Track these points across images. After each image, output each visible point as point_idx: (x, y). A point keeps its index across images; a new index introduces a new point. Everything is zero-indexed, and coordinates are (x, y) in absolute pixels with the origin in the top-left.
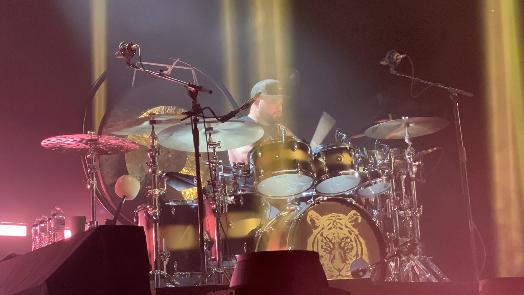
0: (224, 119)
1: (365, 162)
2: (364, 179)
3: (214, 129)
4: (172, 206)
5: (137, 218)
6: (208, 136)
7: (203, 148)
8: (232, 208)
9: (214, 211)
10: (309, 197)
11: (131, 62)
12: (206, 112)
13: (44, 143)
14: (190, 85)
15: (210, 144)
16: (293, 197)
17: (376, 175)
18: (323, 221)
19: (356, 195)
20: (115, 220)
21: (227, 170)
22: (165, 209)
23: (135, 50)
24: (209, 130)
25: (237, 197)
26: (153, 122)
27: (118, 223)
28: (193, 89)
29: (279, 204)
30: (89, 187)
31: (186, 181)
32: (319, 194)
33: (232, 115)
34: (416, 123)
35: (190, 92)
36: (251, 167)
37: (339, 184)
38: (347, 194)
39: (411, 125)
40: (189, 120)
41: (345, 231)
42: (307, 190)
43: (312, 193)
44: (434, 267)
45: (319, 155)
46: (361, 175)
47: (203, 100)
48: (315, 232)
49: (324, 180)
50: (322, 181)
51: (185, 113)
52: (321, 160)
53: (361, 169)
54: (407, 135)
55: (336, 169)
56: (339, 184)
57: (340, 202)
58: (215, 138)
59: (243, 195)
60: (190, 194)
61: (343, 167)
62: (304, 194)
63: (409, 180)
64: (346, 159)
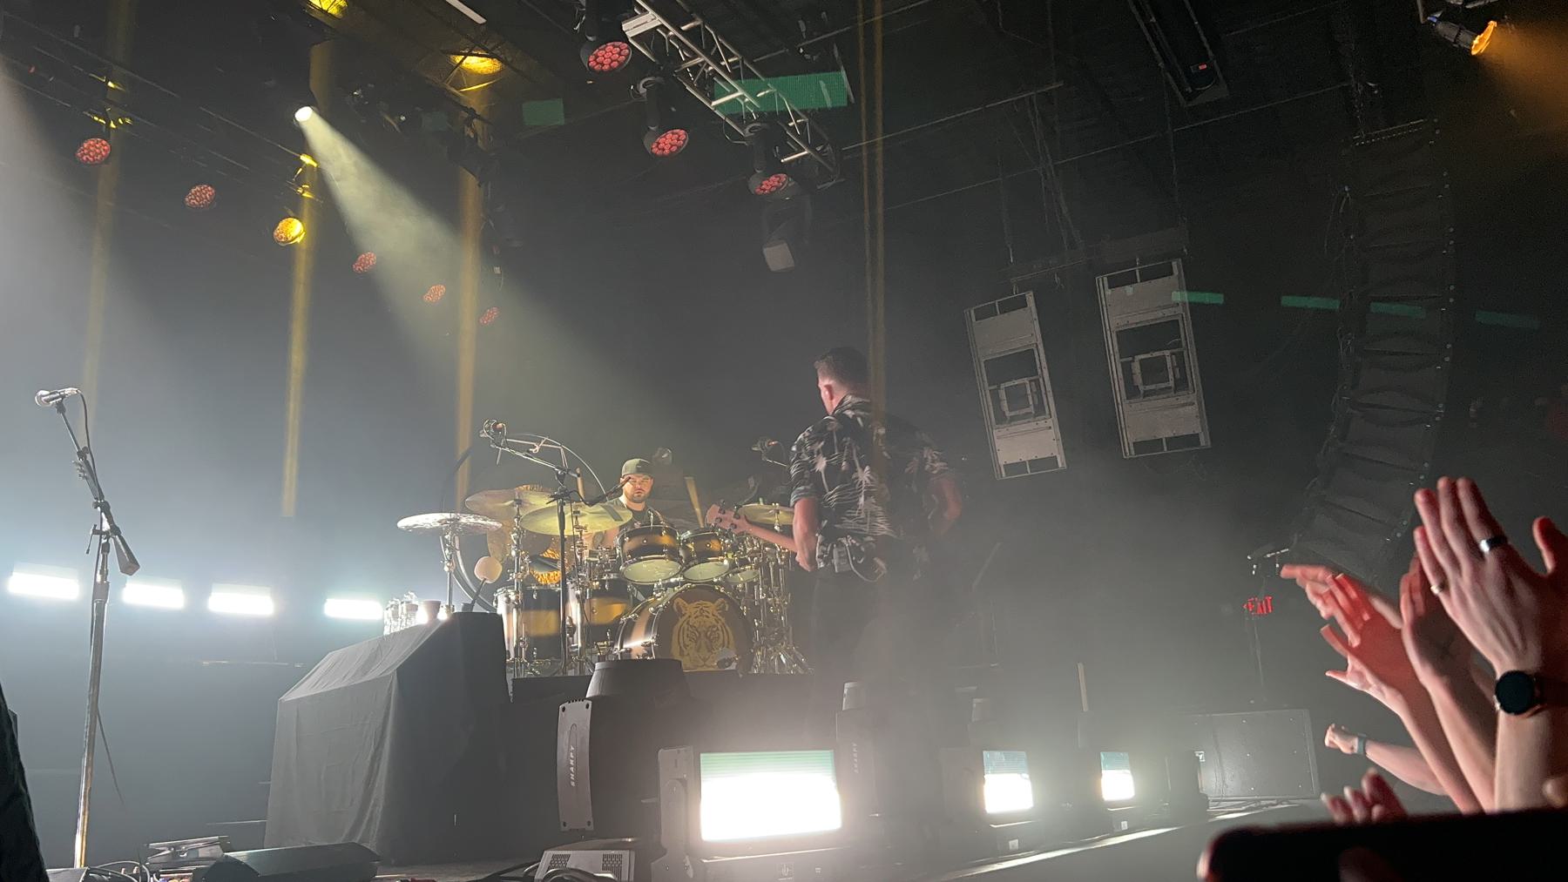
1: (734, 549)
2: (732, 565)
7: (569, 531)
8: (595, 593)
10: (676, 584)
13: (402, 524)
15: (577, 527)
17: (744, 562)
18: (690, 609)
19: (725, 582)
20: (472, 605)
22: (527, 593)
24: (576, 513)
25: (602, 583)
27: (477, 609)
29: (648, 590)
31: (549, 564)
37: (707, 571)
41: (712, 619)
43: (680, 579)
45: (688, 541)
48: (681, 620)
55: (704, 556)
56: (707, 571)
57: (706, 590)
58: (582, 521)
60: (549, 578)
61: (713, 554)
63: (777, 567)
64: (715, 545)
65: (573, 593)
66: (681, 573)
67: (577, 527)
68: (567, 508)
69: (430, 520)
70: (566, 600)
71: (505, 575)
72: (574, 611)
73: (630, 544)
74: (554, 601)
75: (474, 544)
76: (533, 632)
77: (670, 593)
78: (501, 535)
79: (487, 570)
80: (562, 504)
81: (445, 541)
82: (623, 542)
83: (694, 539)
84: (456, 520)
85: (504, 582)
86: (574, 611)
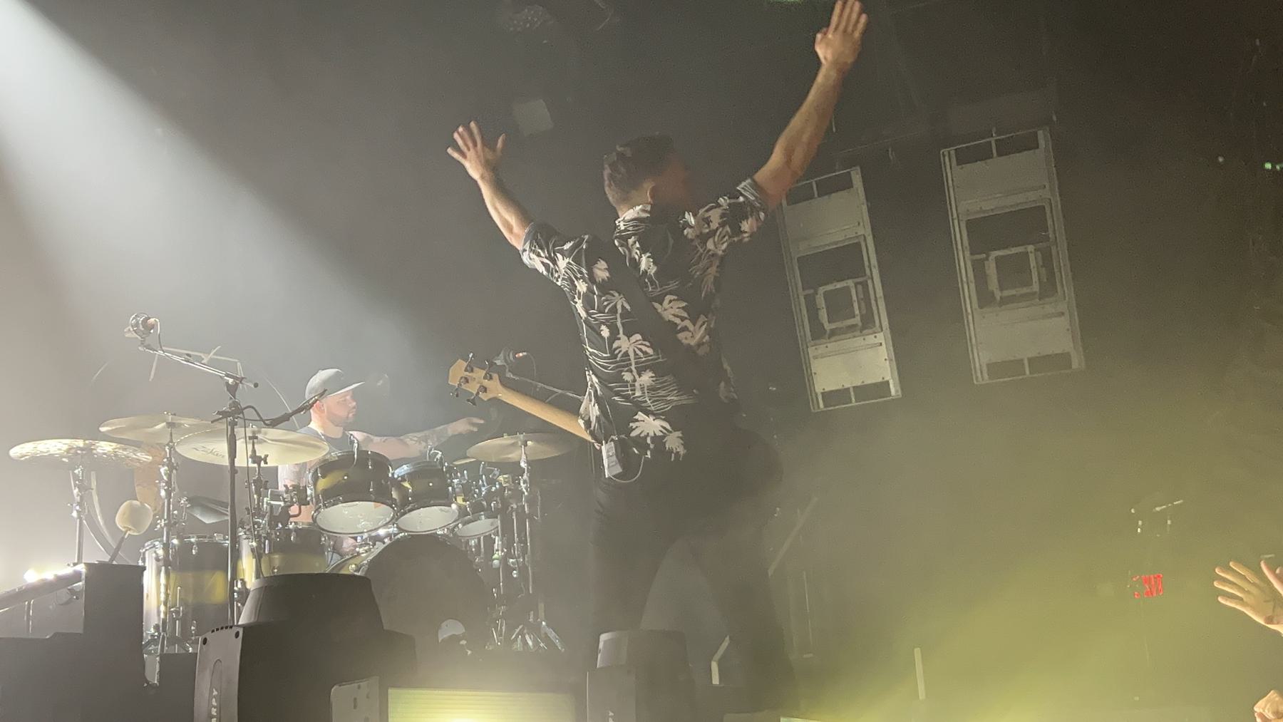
0: (274, 423)
2: (462, 512)
3: (260, 436)
4: (192, 544)
5: (144, 560)
6: (250, 447)
7: (242, 461)
9: (253, 550)
10: (389, 535)
11: (147, 343)
12: (249, 413)
13: (15, 452)
14: (227, 375)
15: (256, 459)
16: (365, 536)
21: (276, 496)
23: (153, 327)
26: (171, 425)
28: (231, 381)
30: (75, 514)
32: (401, 530)
33: (286, 418)
34: (537, 441)
35: (227, 383)
36: (309, 492)
37: (430, 519)
38: (439, 532)
39: (529, 443)
40: (223, 426)
42: (385, 525)
43: (393, 529)
44: (552, 634)
46: (460, 507)
47: (243, 398)
49: (410, 511)
50: (404, 514)
51: (219, 413)
52: (406, 484)
53: (460, 500)
54: (524, 457)
56: (430, 519)
57: (430, 540)
59: (297, 530)
62: (382, 532)
65: (247, 546)
66: (394, 521)
67: (256, 459)
68: (239, 431)
69: (55, 446)
70: (237, 556)
71: (154, 524)
72: (248, 566)
73: (323, 484)
74: (225, 559)
75: (119, 481)
76: (190, 600)
77: (380, 547)
78: (152, 468)
79: (135, 516)
80: (233, 424)
81: (76, 477)
82: (316, 479)
83: (411, 477)
84: (88, 450)
85: (152, 534)
86: (248, 566)
